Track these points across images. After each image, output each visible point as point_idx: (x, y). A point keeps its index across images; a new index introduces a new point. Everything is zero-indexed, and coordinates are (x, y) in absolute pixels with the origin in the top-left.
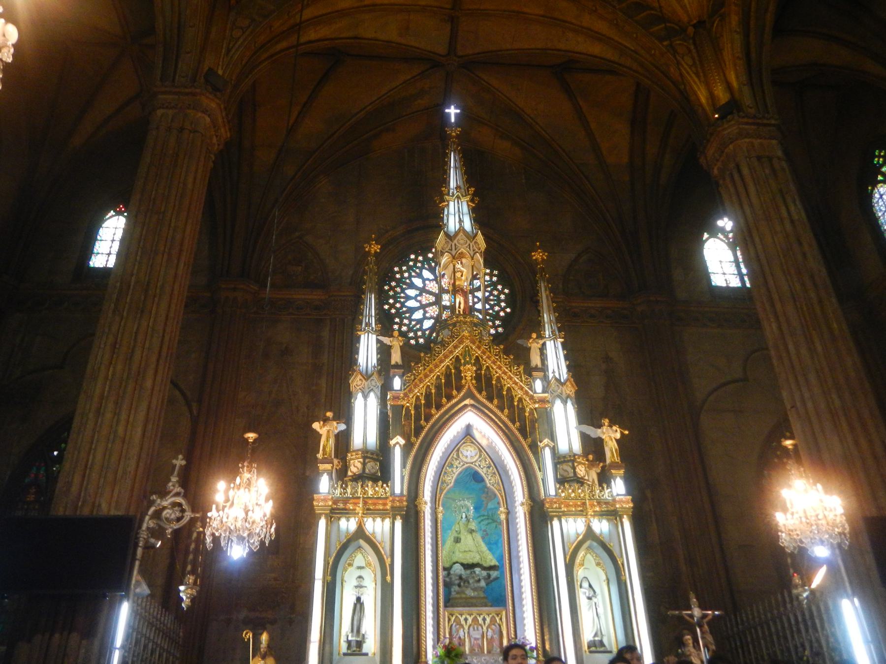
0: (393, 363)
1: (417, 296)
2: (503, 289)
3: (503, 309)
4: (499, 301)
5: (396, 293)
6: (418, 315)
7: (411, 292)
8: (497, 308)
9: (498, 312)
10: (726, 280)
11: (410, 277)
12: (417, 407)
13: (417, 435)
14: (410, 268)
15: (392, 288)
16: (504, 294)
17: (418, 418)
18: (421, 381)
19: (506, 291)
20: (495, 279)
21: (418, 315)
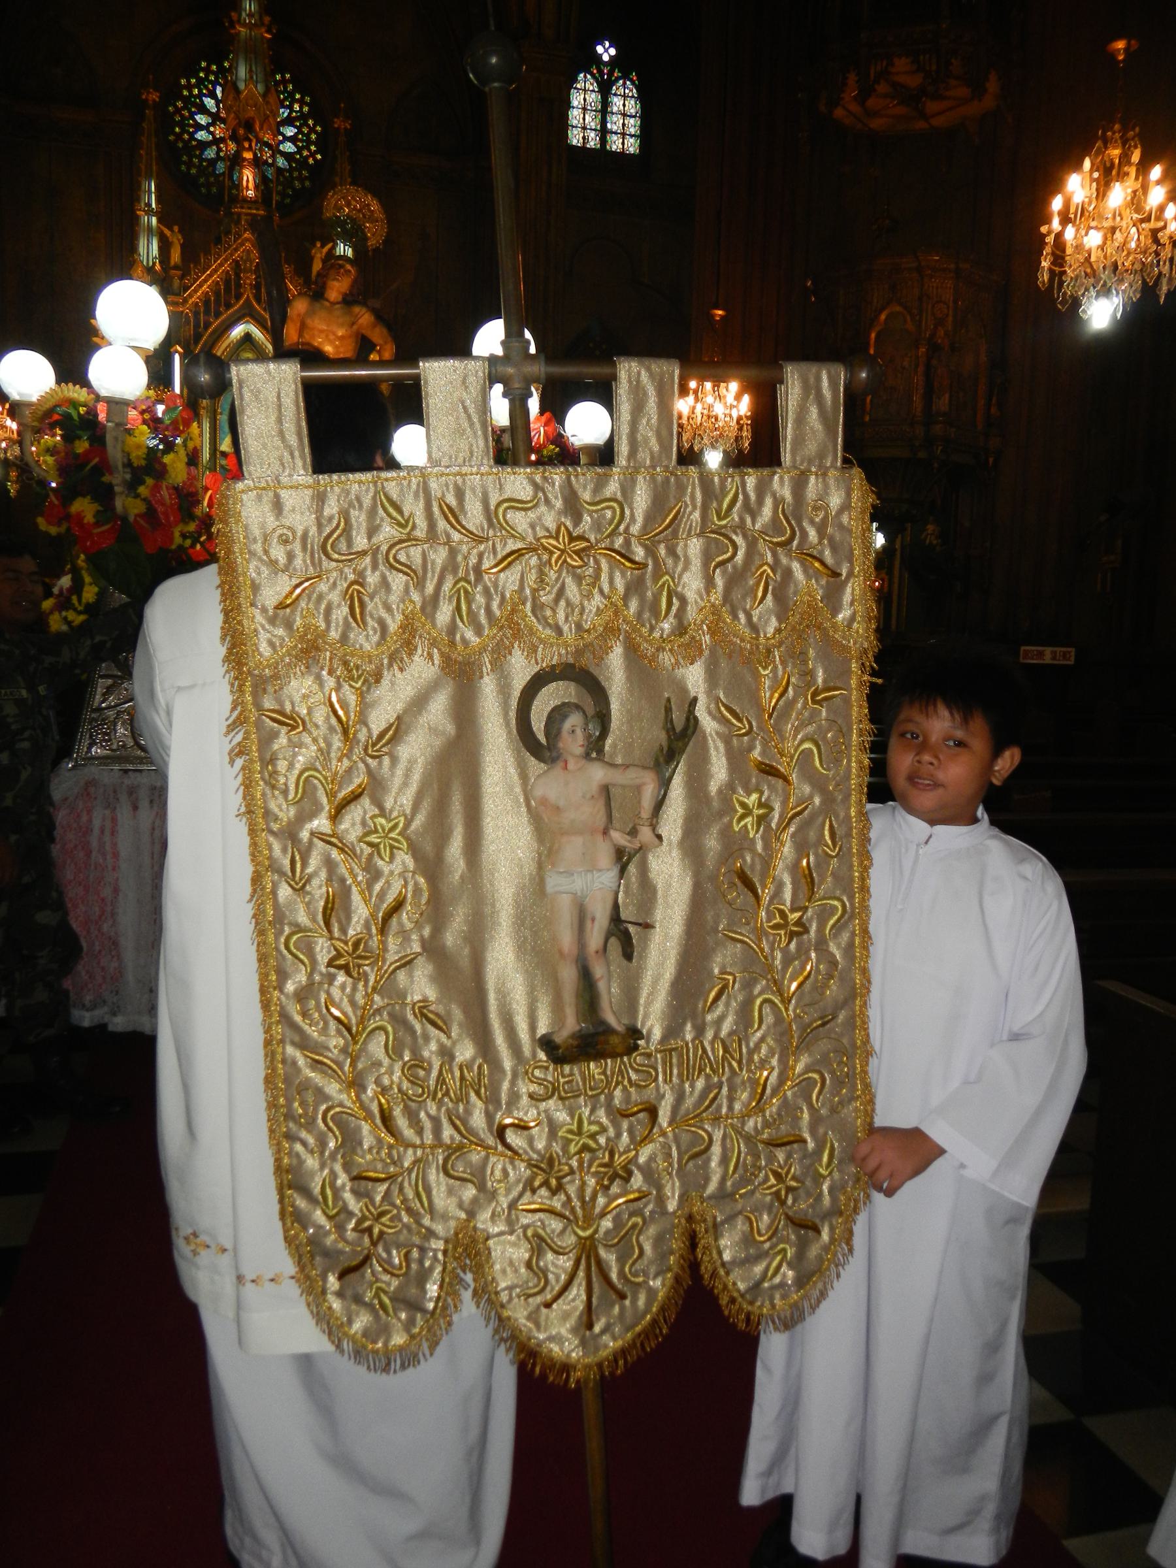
0: (172, 263)
1: (209, 125)
2: (315, 125)
3: (313, 155)
4: (309, 142)
5: (182, 116)
6: (210, 153)
7: (202, 119)
8: (305, 153)
9: (307, 157)
10: (584, 138)
11: (201, 95)
12: (196, 314)
13: (196, 342)
14: (200, 82)
15: (178, 111)
16: (316, 132)
17: (197, 326)
18: (200, 286)
19: (318, 128)
20: (306, 109)
21: (210, 153)
